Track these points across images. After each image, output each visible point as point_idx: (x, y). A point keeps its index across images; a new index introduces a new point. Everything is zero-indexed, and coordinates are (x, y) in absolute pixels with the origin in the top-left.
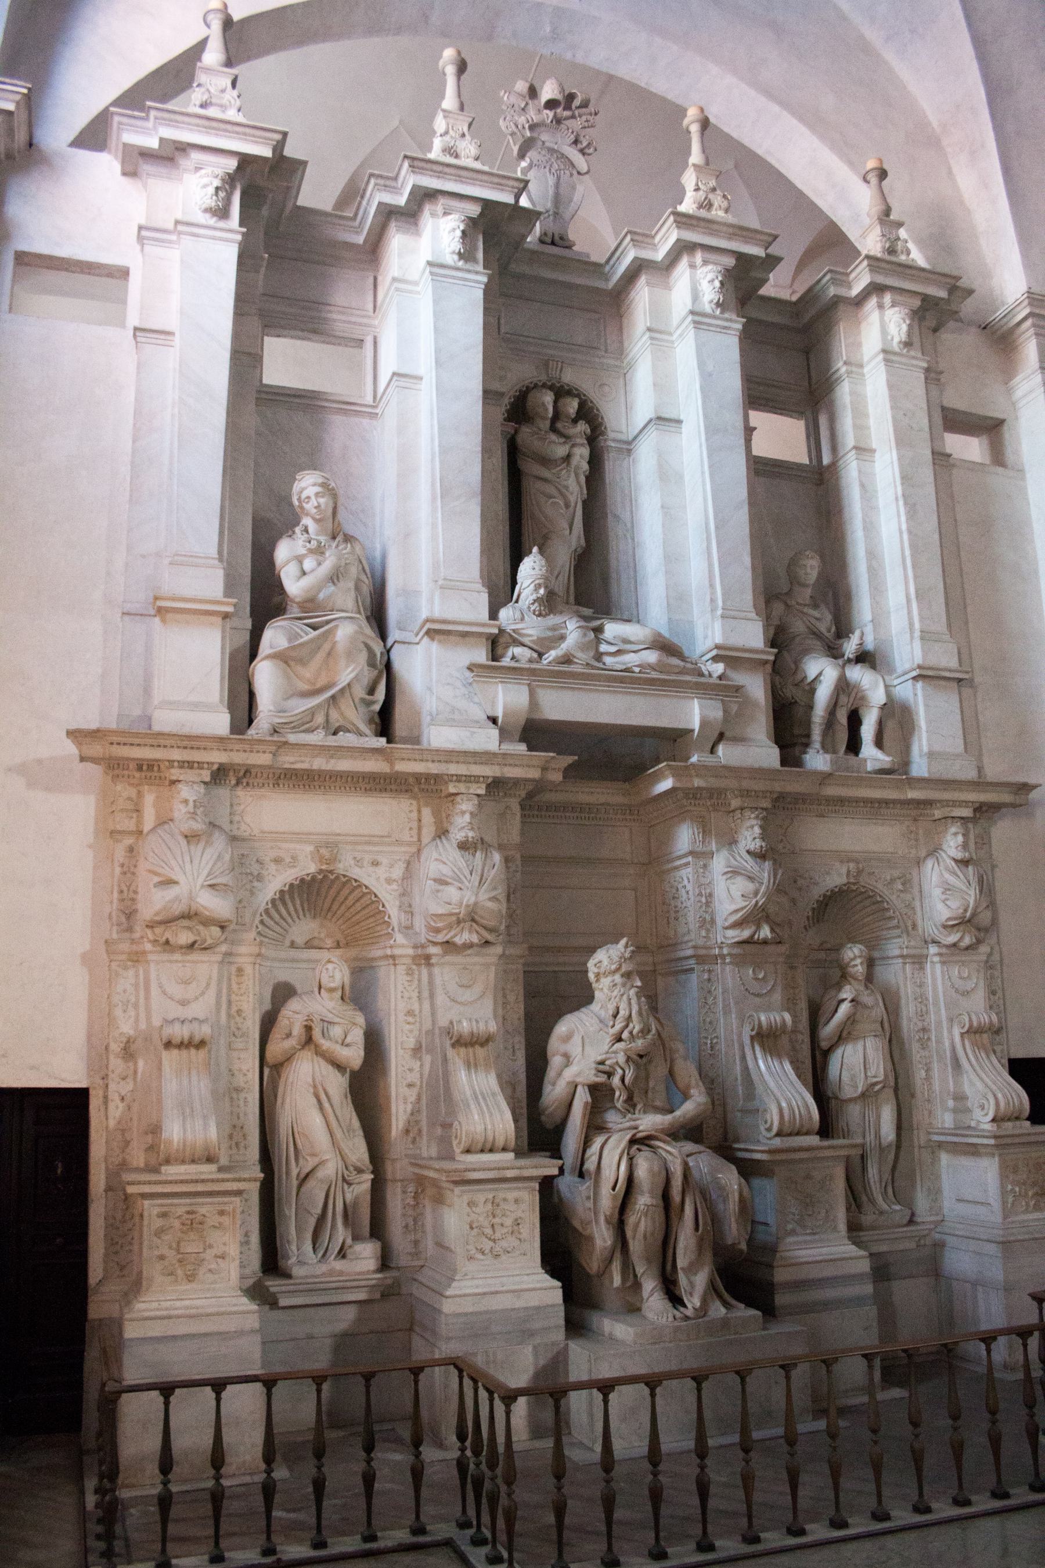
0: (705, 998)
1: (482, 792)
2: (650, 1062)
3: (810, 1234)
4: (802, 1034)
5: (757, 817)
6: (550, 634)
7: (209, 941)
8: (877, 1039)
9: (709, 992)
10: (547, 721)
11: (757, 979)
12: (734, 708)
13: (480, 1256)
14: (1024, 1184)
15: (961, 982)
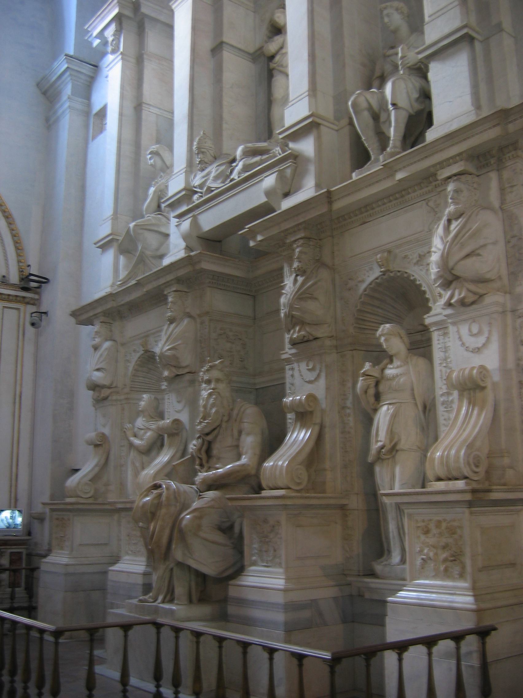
0: (290, 389)
1: (174, 289)
2: (216, 436)
3: (265, 566)
4: (349, 408)
5: (298, 247)
6: (204, 180)
7: (102, 395)
8: (390, 407)
9: (292, 384)
10: (207, 231)
11: (309, 370)
12: (289, 172)
13: (130, 552)
14: (434, 547)
15: (473, 339)
